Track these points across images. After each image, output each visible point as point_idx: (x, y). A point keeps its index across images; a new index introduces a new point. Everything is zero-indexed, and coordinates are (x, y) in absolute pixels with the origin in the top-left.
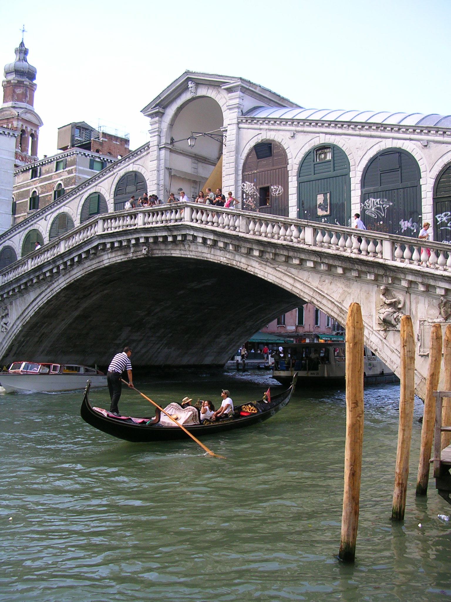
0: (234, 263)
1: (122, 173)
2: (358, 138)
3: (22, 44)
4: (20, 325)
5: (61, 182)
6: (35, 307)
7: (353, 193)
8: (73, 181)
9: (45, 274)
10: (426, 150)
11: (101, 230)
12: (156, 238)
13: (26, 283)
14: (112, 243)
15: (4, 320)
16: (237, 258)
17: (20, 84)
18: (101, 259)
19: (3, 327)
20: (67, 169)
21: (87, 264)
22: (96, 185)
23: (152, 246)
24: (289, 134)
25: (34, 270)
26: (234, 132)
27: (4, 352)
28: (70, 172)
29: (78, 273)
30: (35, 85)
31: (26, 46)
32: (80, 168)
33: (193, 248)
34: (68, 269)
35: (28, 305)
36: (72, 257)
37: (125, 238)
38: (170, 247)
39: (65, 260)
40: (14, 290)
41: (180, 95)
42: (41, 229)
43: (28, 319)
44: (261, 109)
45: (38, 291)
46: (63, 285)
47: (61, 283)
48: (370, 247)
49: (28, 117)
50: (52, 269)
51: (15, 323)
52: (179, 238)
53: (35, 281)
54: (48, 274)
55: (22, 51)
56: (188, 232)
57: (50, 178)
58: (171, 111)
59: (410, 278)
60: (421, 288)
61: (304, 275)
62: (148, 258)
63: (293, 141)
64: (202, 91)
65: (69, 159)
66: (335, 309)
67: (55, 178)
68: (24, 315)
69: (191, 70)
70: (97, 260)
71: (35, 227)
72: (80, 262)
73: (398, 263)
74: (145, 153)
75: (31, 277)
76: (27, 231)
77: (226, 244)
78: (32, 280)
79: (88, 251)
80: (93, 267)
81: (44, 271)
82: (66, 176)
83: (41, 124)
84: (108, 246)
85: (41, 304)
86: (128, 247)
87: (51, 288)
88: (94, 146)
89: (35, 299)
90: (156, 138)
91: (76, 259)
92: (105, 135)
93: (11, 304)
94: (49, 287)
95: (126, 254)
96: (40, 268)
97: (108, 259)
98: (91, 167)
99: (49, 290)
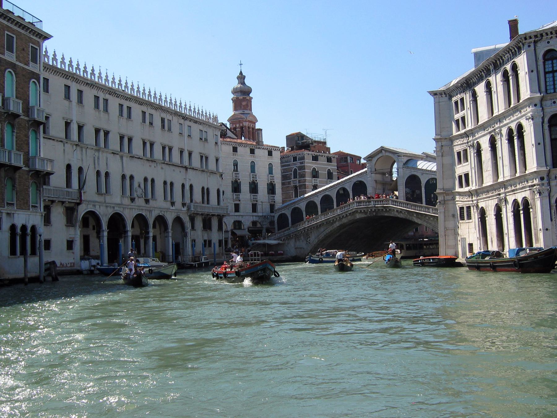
3: (241, 73)
12: (379, 210)
21: (349, 217)
28: (302, 163)
29: (345, 221)
42: (315, 201)
44: (410, 161)
46: (338, 225)
47: (337, 224)
49: (250, 118)
55: (241, 78)
57: (289, 165)
58: (375, 160)
64: (387, 154)
76: (307, 201)
82: (299, 165)
83: (257, 121)
85: (327, 232)
92: (315, 142)
97: (358, 216)
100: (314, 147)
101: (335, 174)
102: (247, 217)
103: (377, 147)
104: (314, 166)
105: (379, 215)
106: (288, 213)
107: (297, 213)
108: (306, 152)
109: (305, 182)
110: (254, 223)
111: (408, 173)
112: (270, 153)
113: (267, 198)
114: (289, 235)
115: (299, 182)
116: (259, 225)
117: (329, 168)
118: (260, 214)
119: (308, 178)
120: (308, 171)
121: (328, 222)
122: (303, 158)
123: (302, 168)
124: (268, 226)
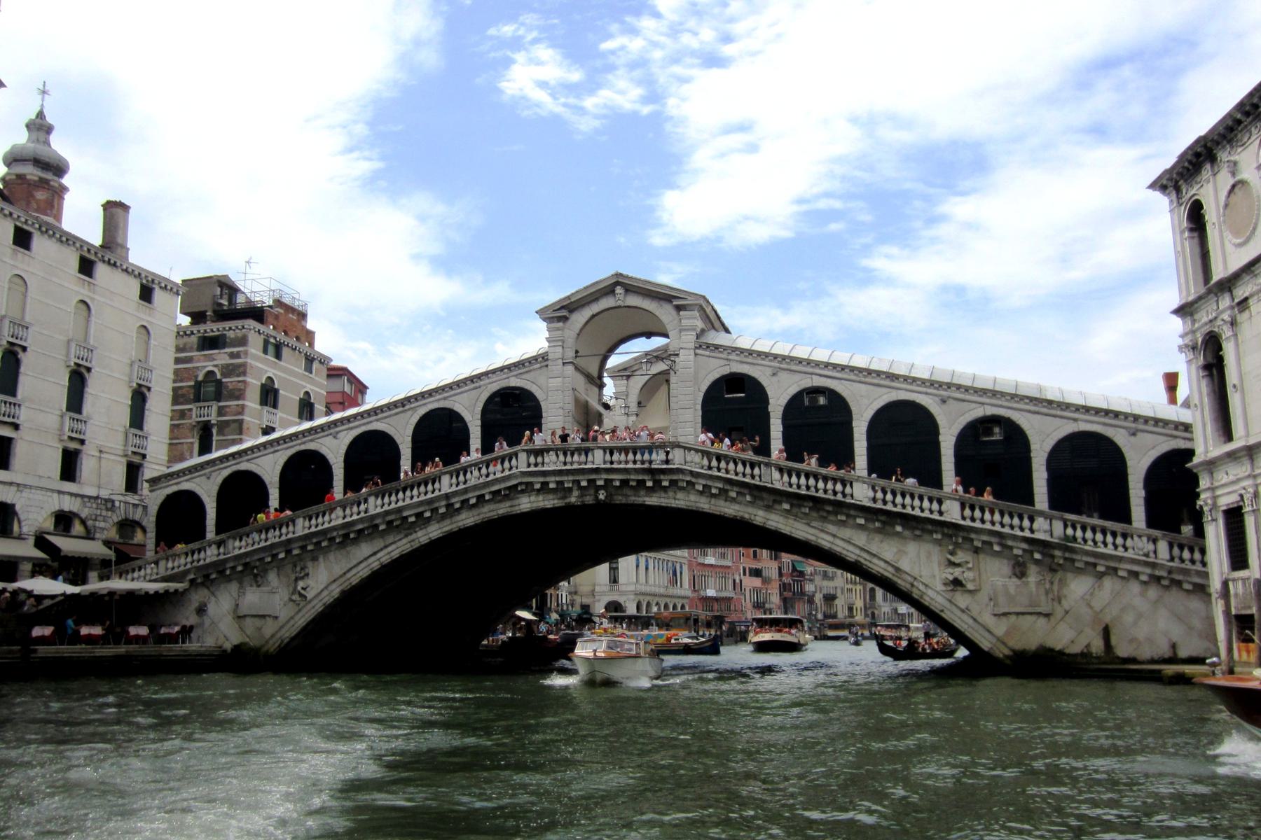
0: (747, 516)
1: (495, 387)
2: (863, 386)
3: (41, 115)
4: (338, 590)
5: (216, 370)
6: (374, 564)
7: (856, 444)
8: (241, 370)
9: (406, 518)
10: (944, 407)
11: (525, 465)
13: (360, 532)
14: (545, 484)
15: (301, 584)
16: (751, 510)
17: (43, 183)
18: (516, 502)
19: (295, 591)
20: (228, 350)
22: (445, 399)
23: (613, 491)
24: (769, 371)
25: (387, 513)
26: (692, 357)
27: (294, 631)
28: (232, 356)
29: (467, 519)
30: (64, 189)
31: (50, 119)
32: (253, 351)
33: (680, 495)
34: (451, 511)
35: (355, 562)
36: (465, 497)
37: (571, 478)
38: (642, 493)
39: (453, 500)
40: (332, 539)
41: (596, 300)
42: (324, 451)
43: (355, 581)
45: (379, 543)
48: (935, 506)
50: (422, 513)
51: (326, 588)
52: (666, 483)
53: (382, 527)
54: (412, 519)
55: (40, 127)
56: (681, 477)
57: (189, 360)
59: (985, 538)
60: (996, 548)
61: (847, 533)
62: (599, 503)
63: (775, 379)
64: (633, 300)
65: (231, 334)
66: (890, 569)
67: (199, 361)
68: (349, 575)
69: (625, 273)
70: (508, 504)
71: (312, 446)
72: (474, 506)
73: (968, 523)
74: (538, 366)
75: (378, 521)
77: (738, 493)
78: (377, 526)
79: (499, 491)
80: (501, 512)
81: (405, 514)
84: (538, 486)
86: (570, 490)
87: (410, 538)
88: (270, 319)
89: (375, 554)
90: (560, 349)
91: (473, 501)
93: (315, 559)
94: (406, 536)
95: (564, 498)
96: (399, 510)
97: (526, 504)
98: (265, 351)
99: (404, 541)
100: (277, 317)
101: (319, 407)
102: (38, 496)
103: (600, 273)
104: (271, 372)
105: (619, 499)
106: (207, 490)
107: (242, 494)
108: (251, 323)
109: (241, 413)
110: (64, 521)
111: (716, 369)
112: (146, 294)
113: (121, 438)
114: (219, 567)
115: (221, 412)
116: (78, 528)
117: (309, 388)
118: (92, 492)
119: (252, 402)
120: (254, 384)
121: (397, 523)
122: (243, 341)
123: (240, 370)
124: (113, 534)
